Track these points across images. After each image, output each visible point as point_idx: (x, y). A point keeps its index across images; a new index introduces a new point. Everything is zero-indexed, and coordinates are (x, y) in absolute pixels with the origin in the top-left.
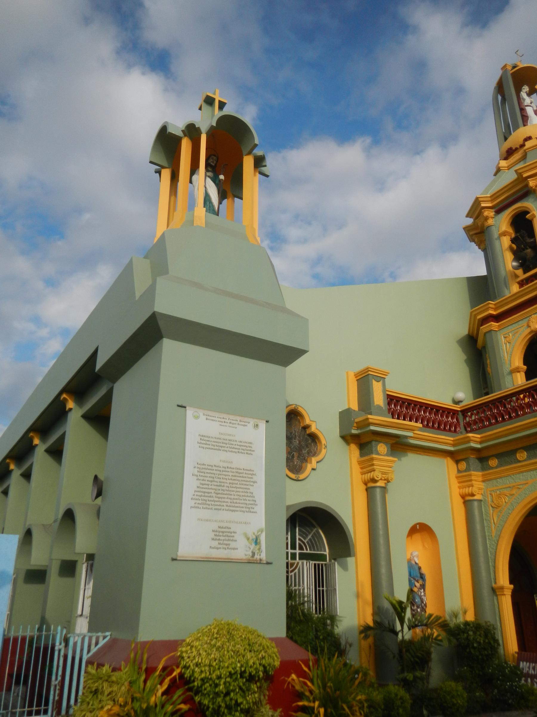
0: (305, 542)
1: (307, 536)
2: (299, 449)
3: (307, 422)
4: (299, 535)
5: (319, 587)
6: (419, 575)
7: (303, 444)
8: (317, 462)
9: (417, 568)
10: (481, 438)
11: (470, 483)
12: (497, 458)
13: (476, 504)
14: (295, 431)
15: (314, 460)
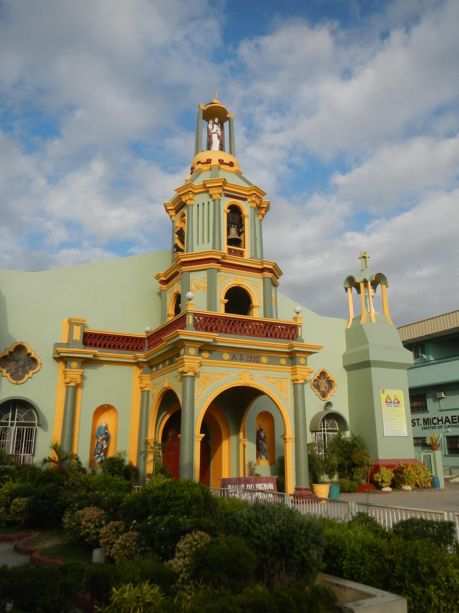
0: (22, 416)
1: (23, 413)
2: (24, 367)
3: (29, 351)
4: (18, 413)
5: (28, 439)
6: (104, 433)
7: (26, 363)
8: (33, 374)
9: (104, 429)
10: (144, 356)
11: (141, 381)
12: (155, 367)
13: (146, 392)
14: (22, 357)
15: (31, 372)
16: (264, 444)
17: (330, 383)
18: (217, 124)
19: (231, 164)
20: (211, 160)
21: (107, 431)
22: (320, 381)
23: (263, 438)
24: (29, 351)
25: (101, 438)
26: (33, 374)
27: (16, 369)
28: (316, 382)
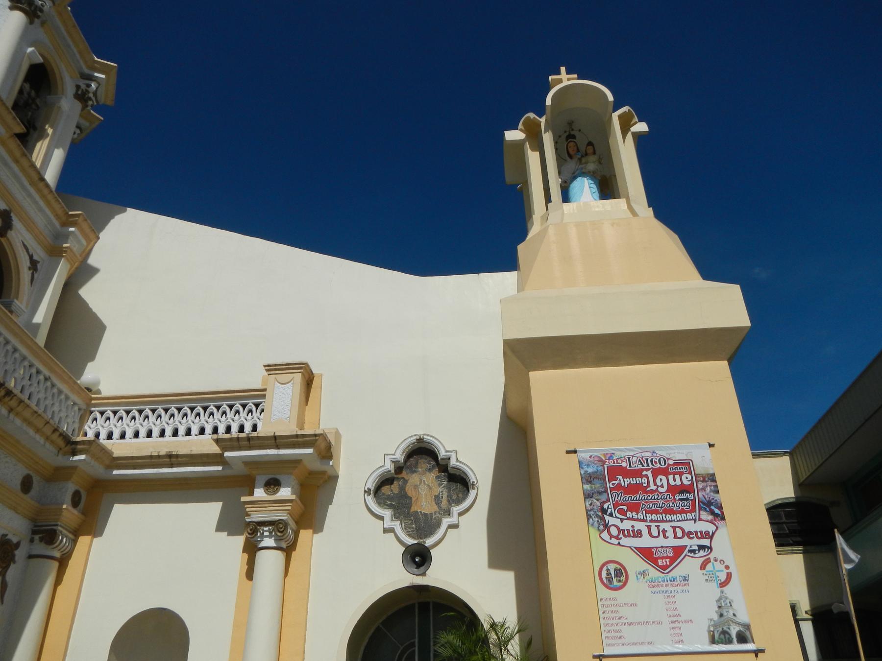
22: (413, 479)
28: (395, 488)
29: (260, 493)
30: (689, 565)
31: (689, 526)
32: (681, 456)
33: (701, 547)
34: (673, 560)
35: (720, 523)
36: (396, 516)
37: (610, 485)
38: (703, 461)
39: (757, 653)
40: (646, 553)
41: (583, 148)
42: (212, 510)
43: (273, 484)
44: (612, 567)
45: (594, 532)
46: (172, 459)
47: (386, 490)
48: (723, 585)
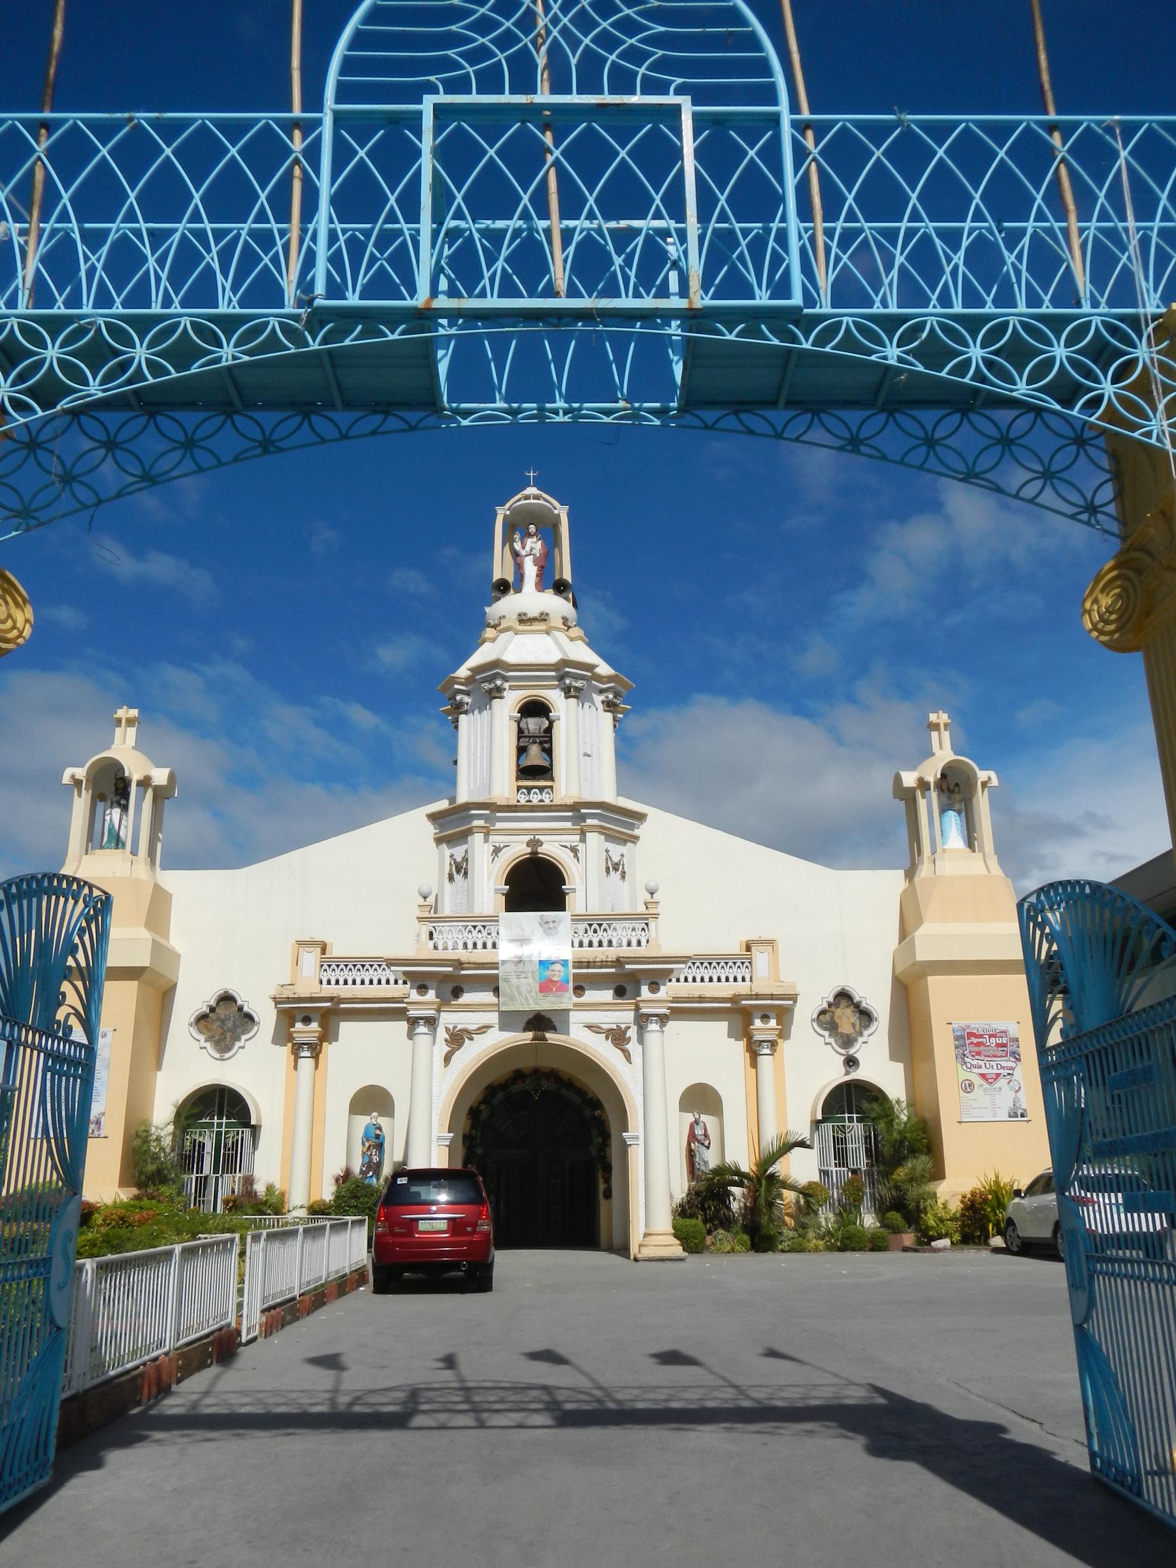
7: (238, 1023)
8: (246, 1040)
15: (244, 1037)
16: (704, 1148)
17: (866, 1016)
18: (535, 534)
19: (543, 618)
20: (504, 617)
21: (378, 1132)
22: (838, 1012)
23: (700, 1138)
24: (239, 1002)
25: (367, 1144)
26: (246, 1040)
27: (222, 1034)
28: (827, 1017)
29: (758, 1023)
30: (1002, 1082)
31: (1004, 1064)
32: (1002, 1028)
33: (1009, 1074)
34: (995, 1079)
35: (1018, 1063)
36: (830, 1035)
37: (967, 1042)
38: (1014, 1030)
39: (1028, 1121)
40: (983, 1076)
41: (952, 787)
42: (722, 1026)
43: (765, 1018)
44: (967, 1082)
45: (959, 1066)
46: (701, 999)
47: (822, 1017)
48: (1016, 1092)
